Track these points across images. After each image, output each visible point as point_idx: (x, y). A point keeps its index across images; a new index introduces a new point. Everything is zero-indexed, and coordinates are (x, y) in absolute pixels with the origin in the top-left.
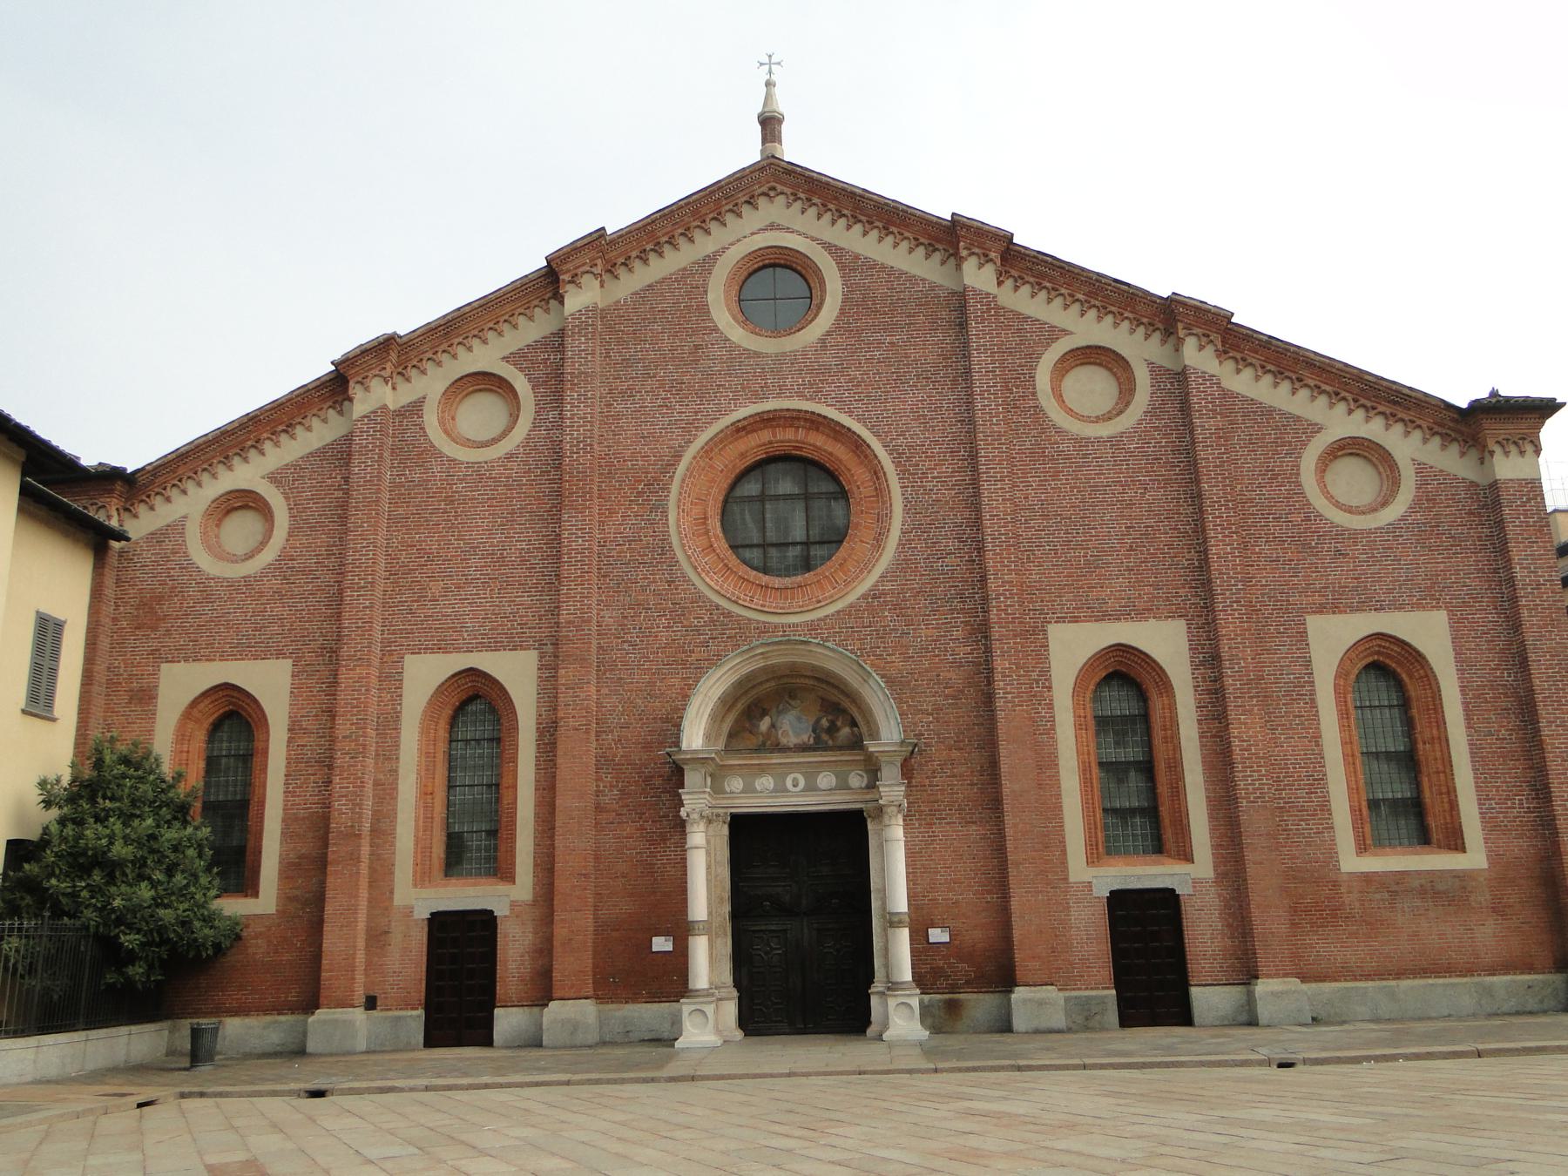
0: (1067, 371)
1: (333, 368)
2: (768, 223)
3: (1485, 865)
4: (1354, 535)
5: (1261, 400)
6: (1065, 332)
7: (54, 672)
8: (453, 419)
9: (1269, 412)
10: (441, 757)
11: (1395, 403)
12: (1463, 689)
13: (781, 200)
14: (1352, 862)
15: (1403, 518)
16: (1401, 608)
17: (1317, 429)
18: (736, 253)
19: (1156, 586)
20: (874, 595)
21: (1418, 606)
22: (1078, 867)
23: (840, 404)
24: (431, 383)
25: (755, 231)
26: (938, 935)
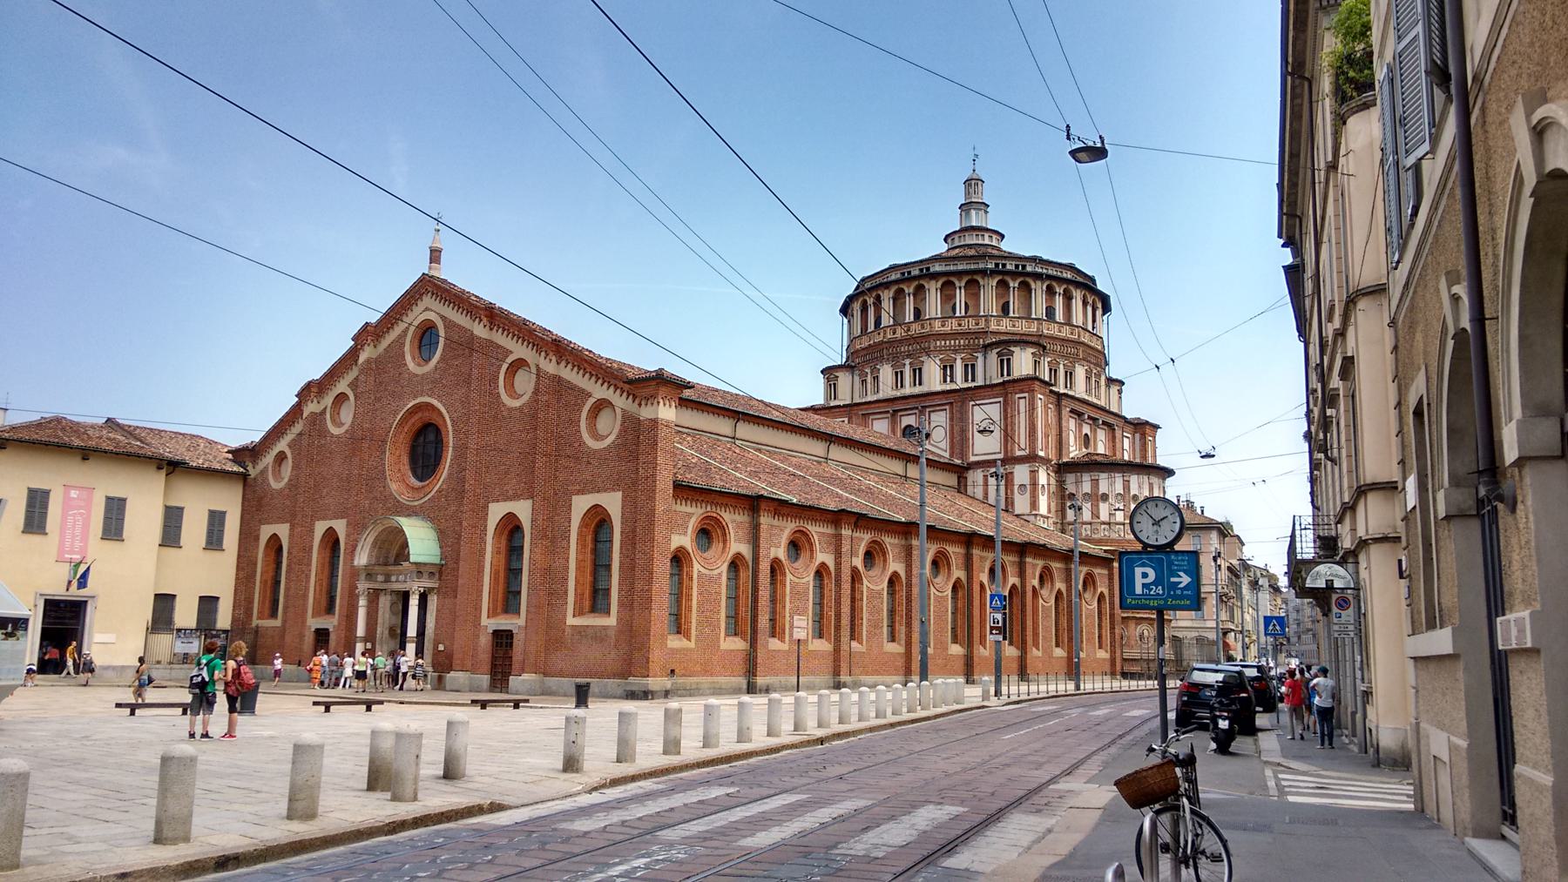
1: (297, 399)
3: (615, 624)
6: (511, 352)
7: (222, 532)
8: (338, 414)
9: (572, 388)
10: (327, 565)
14: (571, 621)
17: (589, 395)
18: (416, 323)
19: (525, 483)
20: (439, 491)
22: (485, 621)
23: (439, 398)
24: (328, 400)
26: (441, 647)
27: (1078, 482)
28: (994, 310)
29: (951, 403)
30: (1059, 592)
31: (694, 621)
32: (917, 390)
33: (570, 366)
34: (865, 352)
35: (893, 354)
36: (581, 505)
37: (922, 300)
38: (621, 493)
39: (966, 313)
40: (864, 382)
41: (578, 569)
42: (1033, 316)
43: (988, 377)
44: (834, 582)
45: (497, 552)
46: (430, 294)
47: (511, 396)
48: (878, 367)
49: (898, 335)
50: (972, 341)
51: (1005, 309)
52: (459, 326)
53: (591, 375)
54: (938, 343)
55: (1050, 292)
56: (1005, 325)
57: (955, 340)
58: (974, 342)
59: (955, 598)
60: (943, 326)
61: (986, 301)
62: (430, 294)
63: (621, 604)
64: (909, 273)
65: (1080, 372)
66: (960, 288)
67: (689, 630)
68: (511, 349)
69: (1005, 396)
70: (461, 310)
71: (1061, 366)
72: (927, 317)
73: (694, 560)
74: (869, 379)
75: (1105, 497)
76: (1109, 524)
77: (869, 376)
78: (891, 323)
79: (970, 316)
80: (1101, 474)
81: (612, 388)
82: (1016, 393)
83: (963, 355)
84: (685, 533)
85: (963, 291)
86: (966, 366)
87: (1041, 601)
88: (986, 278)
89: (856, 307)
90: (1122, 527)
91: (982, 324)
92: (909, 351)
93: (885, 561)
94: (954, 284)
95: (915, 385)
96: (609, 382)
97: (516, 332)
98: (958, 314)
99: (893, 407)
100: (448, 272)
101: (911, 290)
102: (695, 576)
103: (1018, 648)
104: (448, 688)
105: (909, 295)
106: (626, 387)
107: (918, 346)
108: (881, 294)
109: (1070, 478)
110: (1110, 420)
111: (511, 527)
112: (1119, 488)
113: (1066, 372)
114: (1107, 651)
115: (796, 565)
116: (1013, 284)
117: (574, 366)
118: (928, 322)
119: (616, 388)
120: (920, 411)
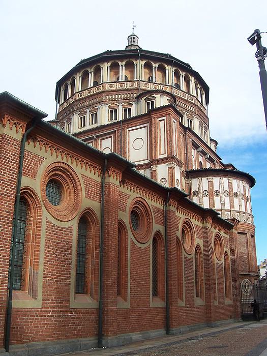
30: (198, 247)
32: (95, 126)
42: (167, 84)
50: (129, 95)
51: (150, 80)
54: (107, 97)
55: (177, 75)
56: (150, 87)
58: (130, 96)
59: (82, 236)
60: (111, 87)
61: (138, 69)
66: (122, 66)
72: (102, 83)
74: (65, 128)
75: (217, 193)
77: (66, 123)
80: (214, 178)
85: (124, 68)
86: (125, 110)
87: (184, 252)
88: (138, 61)
90: (229, 213)
91: (135, 86)
95: (92, 124)
98: (120, 80)
101: (92, 70)
103: (163, 299)
107: (96, 99)
109: (194, 182)
110: (213, 157)
113: (188, 120)
114: (230, 299)
116: (155, 65)
118: (101, 85)
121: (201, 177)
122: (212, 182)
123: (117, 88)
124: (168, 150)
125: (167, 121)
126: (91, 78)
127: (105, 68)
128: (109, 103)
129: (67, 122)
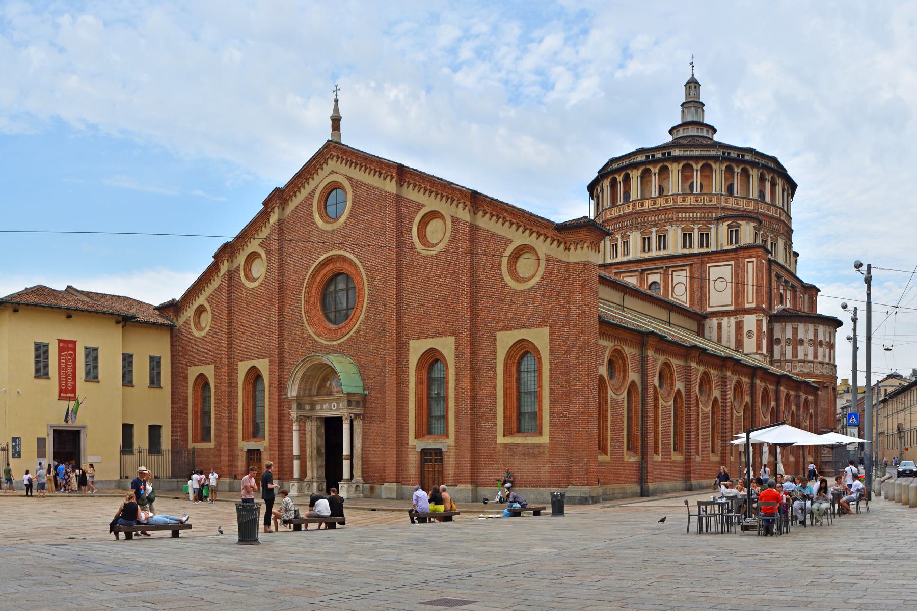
0: (428, 223)
2: (330, 170)
4: (518, 293)
5: (490, 230)
9: (493, 235)
11: (538, 226)
12: (551, 364)
13: (335, 159)
14: (501, 440)
15: (538, 284)
16: (532, 327)
21: (539, 326)
25: (326, 175)
27: (783, 331)
28: (723, 190)
29: (691, 265)
31: (609, 438)
33: (488, 216)
34: (616, 222)
35: (641, 223)
36: (505, 340)
37: (664, 179)
38: (548, 328)
39: (701, 190)
40: (614, 246)
41: (506, 395)
43: (719, 244)
44: (684, 405)
45: (419, 382)
46: (335, 158)
47: (425, 245)
48: (628, 233)
49: (645, 207)
50: (706, 214)
52: (365, 185)
53: (512, 224)
56: (731, 203)
57: (693, 213)
58: (708, 215)
60: (684, 201)
62: (335, 158)
63: (553, 424)
64: (653, 156)
65: (781, 243)
67: (606, 445)
68: (423, 203)
69: (737, 260)
70: (368, 170)
71: (769, 239)
72: (671, 193)
73: (609, 387)
75: (801, 342)
76: (804, 362)
77: (620, 240)
78: (639, 197)
79: (705, 194)
81: (535, 235)
82: (746, 258)
83: (700, 226)
84: (602, 364)
86: (702, 234)
89: (606, 183)
90: (812, 364)
92: (655, 221)
93: (710, 389)
94: (691, 167)
95: (660, 249)
96: (531, 229)
97: (428, 187)
98: (695, 192)
99: (642, 266)
100: (348, 139)
101: (657, 170)
102: (609, 401)
104: (383, 496)
105: (655, 174)
106: (550, 233)
108: (629, 171)
110: (795, 283)
111: (432, 359)
112: (789, 335)
113: (772, 243)
115: (662, 391)
117: (492, 216)
118: (672, 197)
119: (539, 234)
120: (665, 271)
121: (786, 322)
122: (797, 329)
123: (692, 203)
124: (756, 299)
125: (756, 263)
126: (655, 181)
127: (675, 172)
128: (682, 224)
129: (622, 238)
